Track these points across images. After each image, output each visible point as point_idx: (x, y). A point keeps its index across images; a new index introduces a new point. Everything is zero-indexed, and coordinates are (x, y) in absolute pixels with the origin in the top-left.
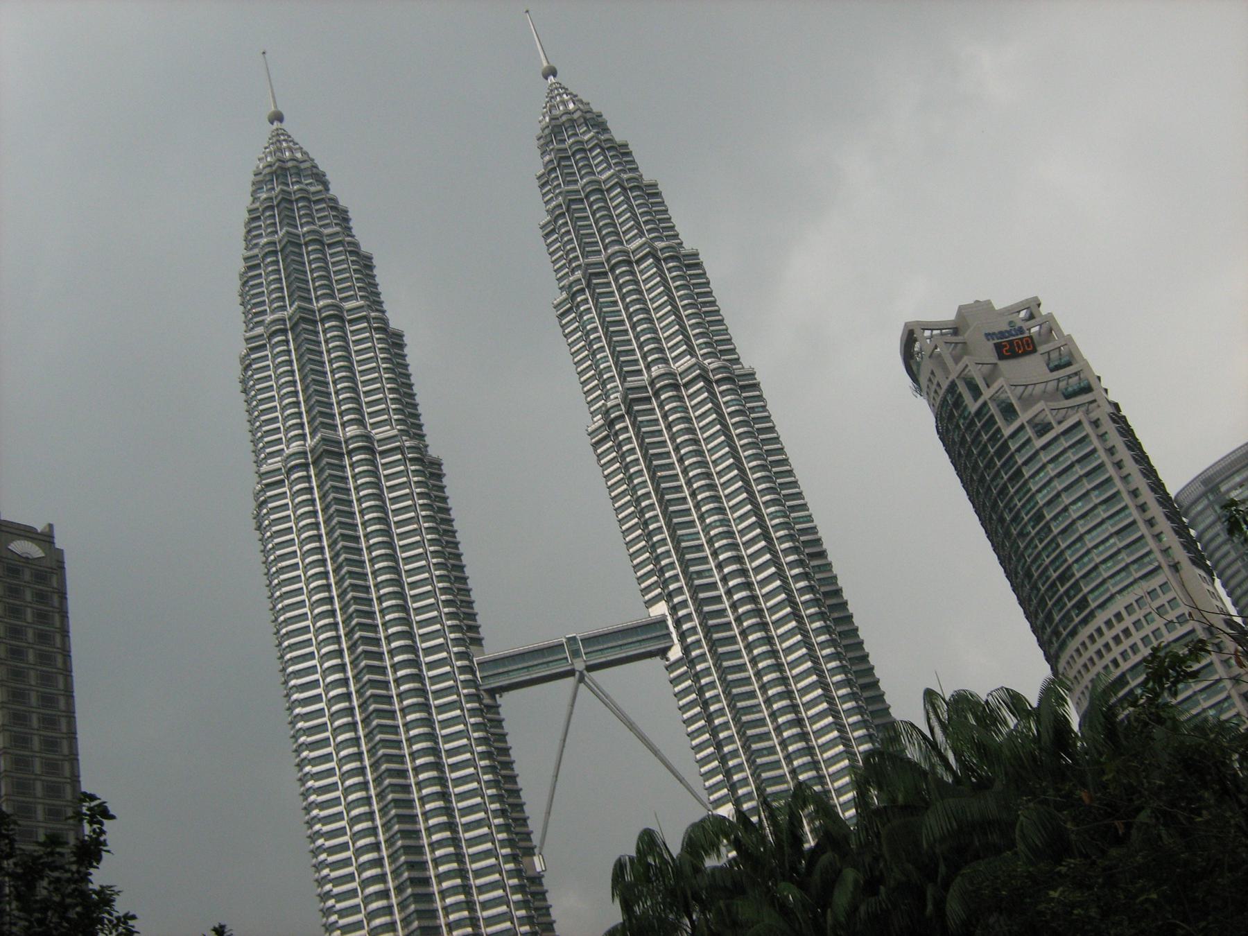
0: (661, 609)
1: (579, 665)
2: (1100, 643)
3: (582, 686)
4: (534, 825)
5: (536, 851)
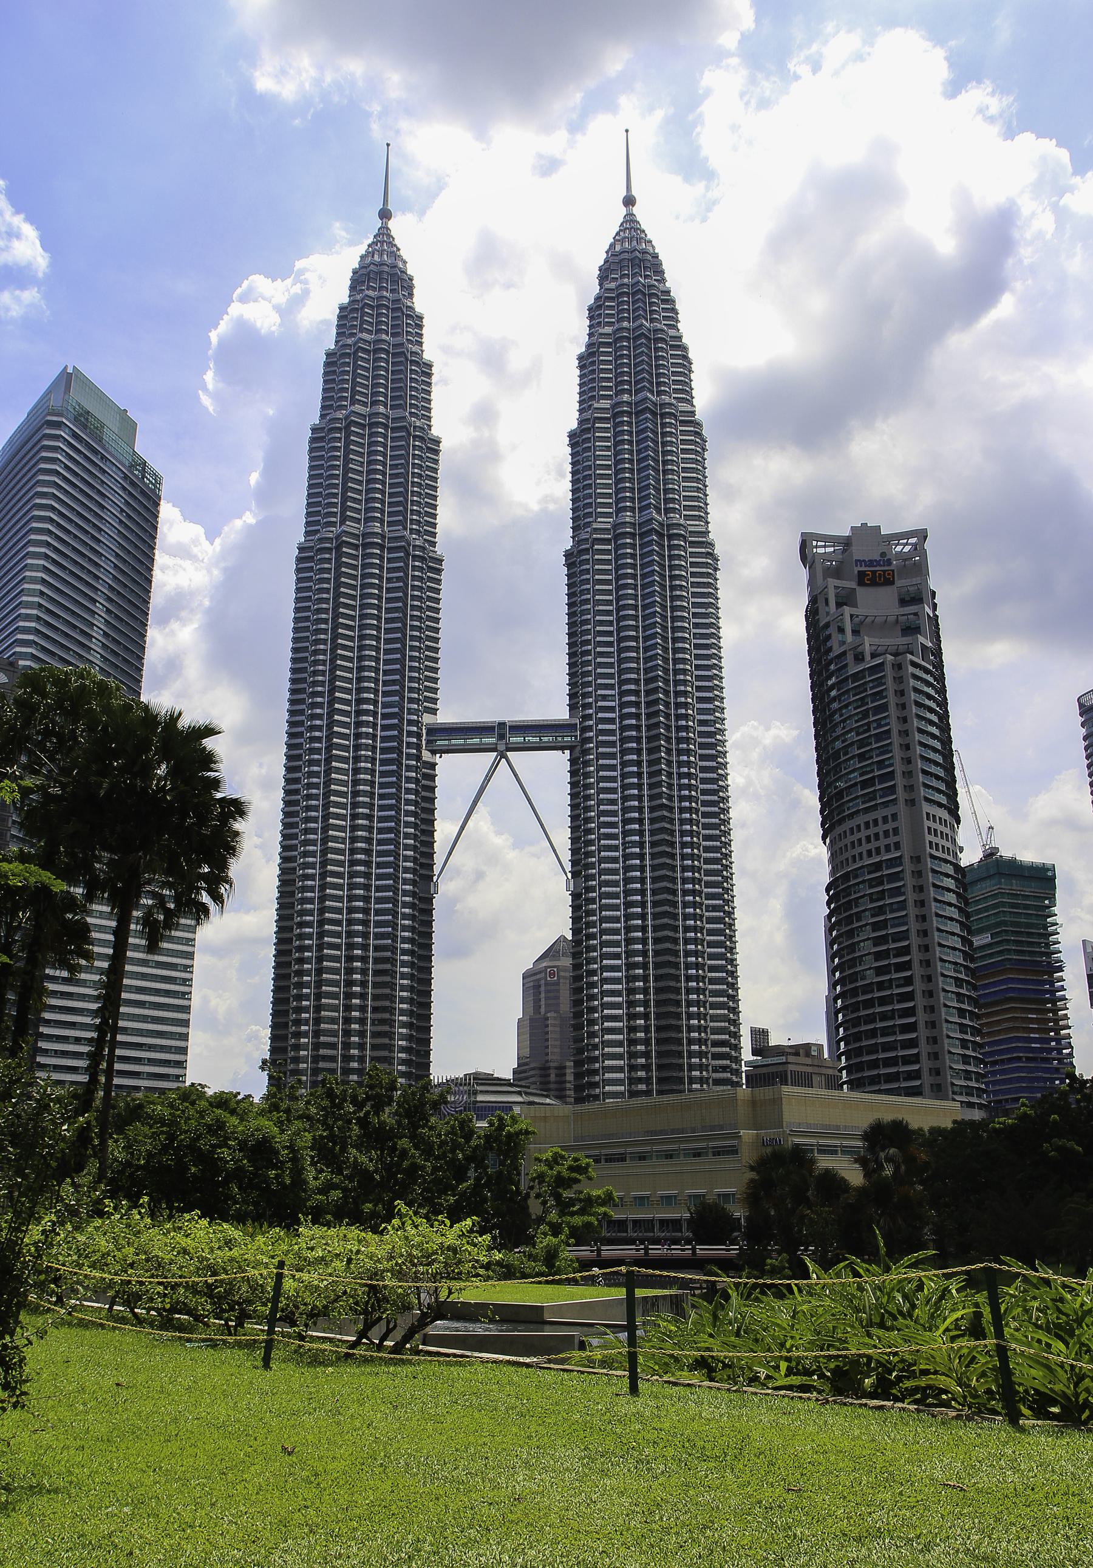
1: (502, 747)
4: (439, 859)
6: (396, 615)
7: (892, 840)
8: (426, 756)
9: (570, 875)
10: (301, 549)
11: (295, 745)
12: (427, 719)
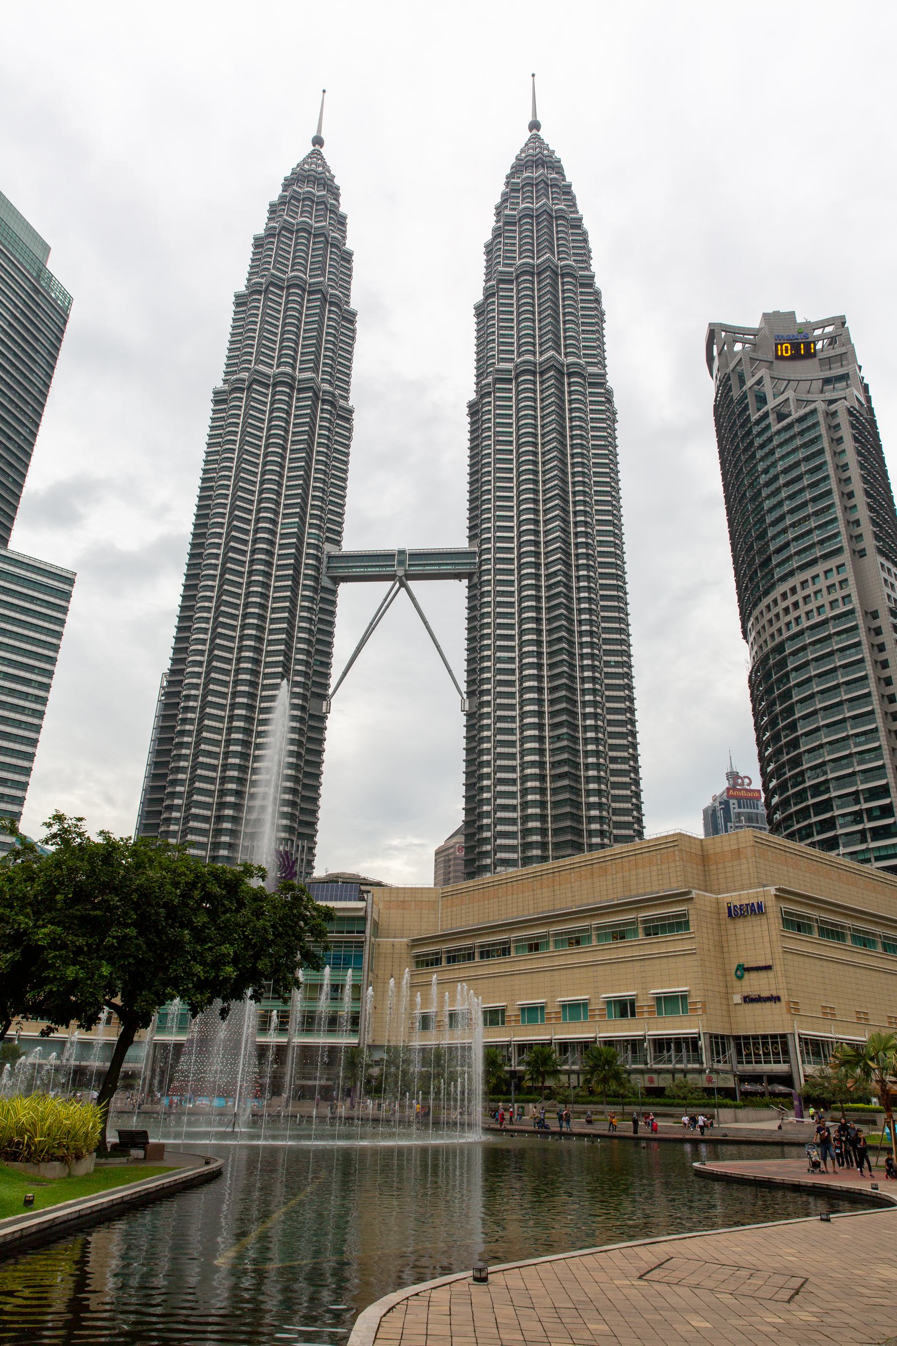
1: (400, 573)
2: (791, 600)
3: (403, 590)
6: (302, 446)
7: (838, 594)
9: (465, 696)
10: (216, 393)
11: (195, 564)
12: (328, 548)
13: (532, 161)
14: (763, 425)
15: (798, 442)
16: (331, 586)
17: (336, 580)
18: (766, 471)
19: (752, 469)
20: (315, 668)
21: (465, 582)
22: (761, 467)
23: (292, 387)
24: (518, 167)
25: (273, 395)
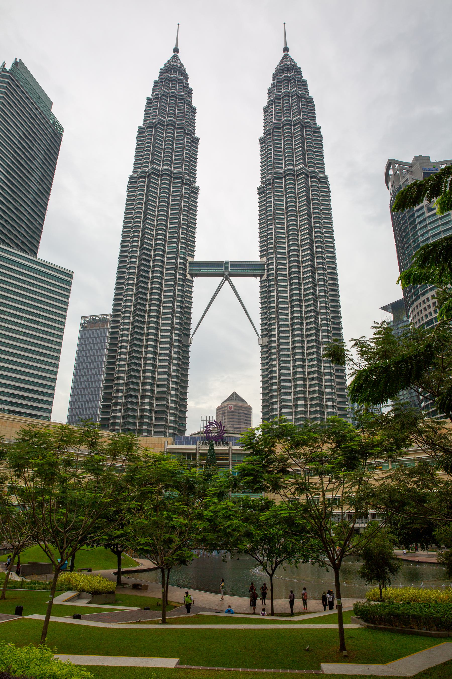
0: (264, 259)
1: (226, 273)
3: (227, 282)
4: (193, 327)
5: (191, 336)
8: (188, 277)
9: (260, 337)
12: (189, 259)
13: (287, 68)
14: (421, 212)
15: (440, 222)
16: (190, 278)
17: (193, 276)
18: (422, 235)
19: (414, 233)
20: (185, 321)
21: (259, 279)
22: (419, 233)
23: (171, 177)
24: (280, 70)
25: (161, 180)
